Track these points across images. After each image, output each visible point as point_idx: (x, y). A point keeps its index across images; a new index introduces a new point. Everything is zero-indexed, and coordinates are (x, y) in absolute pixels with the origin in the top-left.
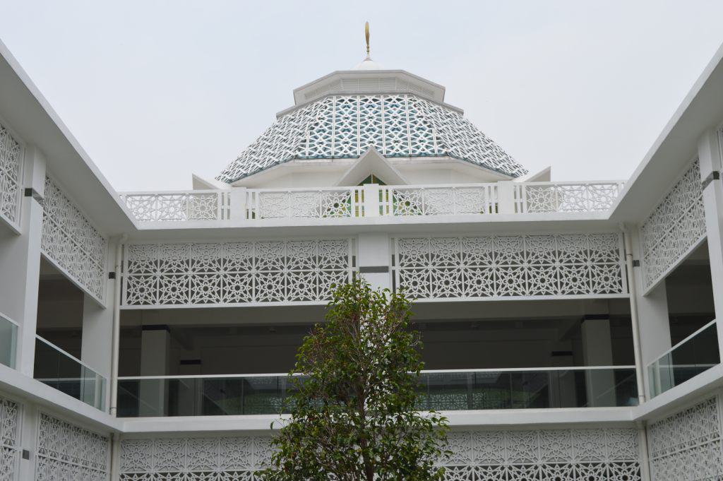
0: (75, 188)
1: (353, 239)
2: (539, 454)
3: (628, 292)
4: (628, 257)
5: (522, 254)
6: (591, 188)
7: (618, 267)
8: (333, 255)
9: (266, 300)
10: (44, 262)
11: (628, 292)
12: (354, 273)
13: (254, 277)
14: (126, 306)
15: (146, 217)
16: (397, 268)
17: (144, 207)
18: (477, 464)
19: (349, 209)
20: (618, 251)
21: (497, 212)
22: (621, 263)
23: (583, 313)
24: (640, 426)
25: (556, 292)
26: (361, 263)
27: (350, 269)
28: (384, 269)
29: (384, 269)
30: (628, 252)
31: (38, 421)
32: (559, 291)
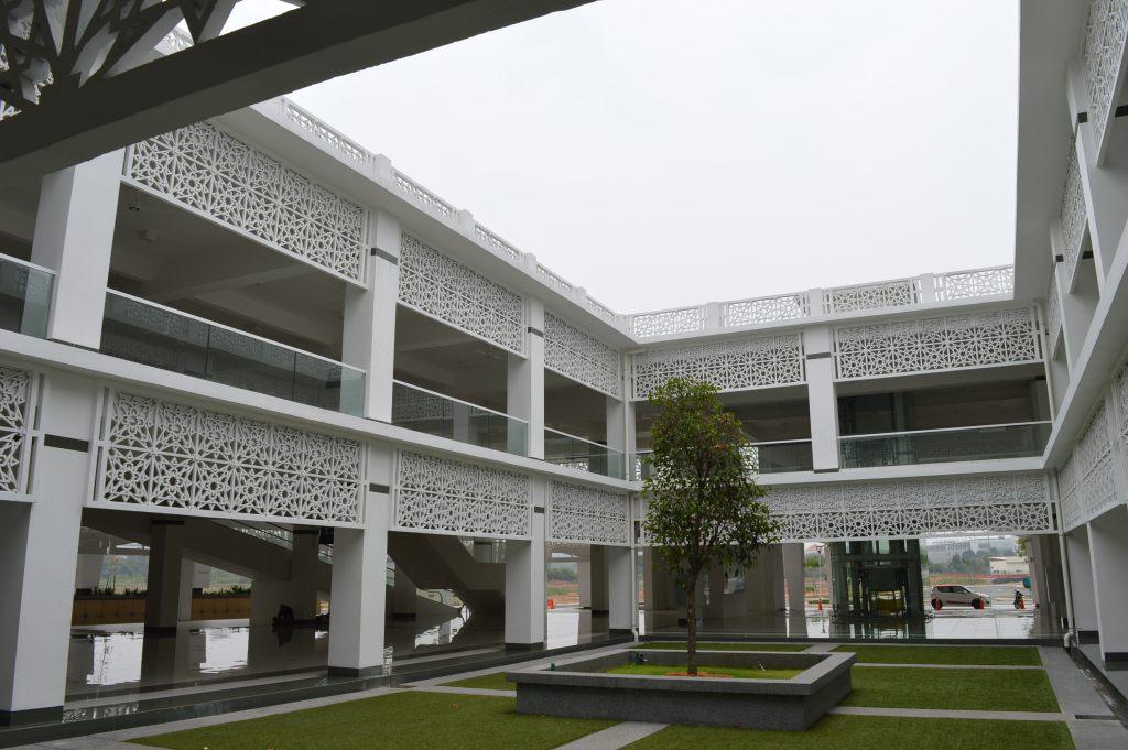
0: (570, 319)
1: (802, 334)
2: (955, 497)
3: (1041, 357)
4: (1041, 327)
5: (889, 339)
6: (1003, 271)
7: (1031, 337)
8: (791, 344)
9: (786, 382)
10: (547, 372)
11: (1041, 357)
12: (804, 360)
13: (727, 369)
14: (636, 399)
15: (642, 334)
16: (838, 354)
17: (691, 318)
18: (932, 506)
19: (909, 296)
20: (1030, 323)
21: (916, 301)
22: (1034, 333)
23: (1034, 375)
24: (1052, 473)
25: (1004, 360)
26: (807, 352)
27: (801, 357)
28: (827, 355)
29: (827, 355)
30: (1040, 322)
31: (549, 487)
32: (895, 370)
